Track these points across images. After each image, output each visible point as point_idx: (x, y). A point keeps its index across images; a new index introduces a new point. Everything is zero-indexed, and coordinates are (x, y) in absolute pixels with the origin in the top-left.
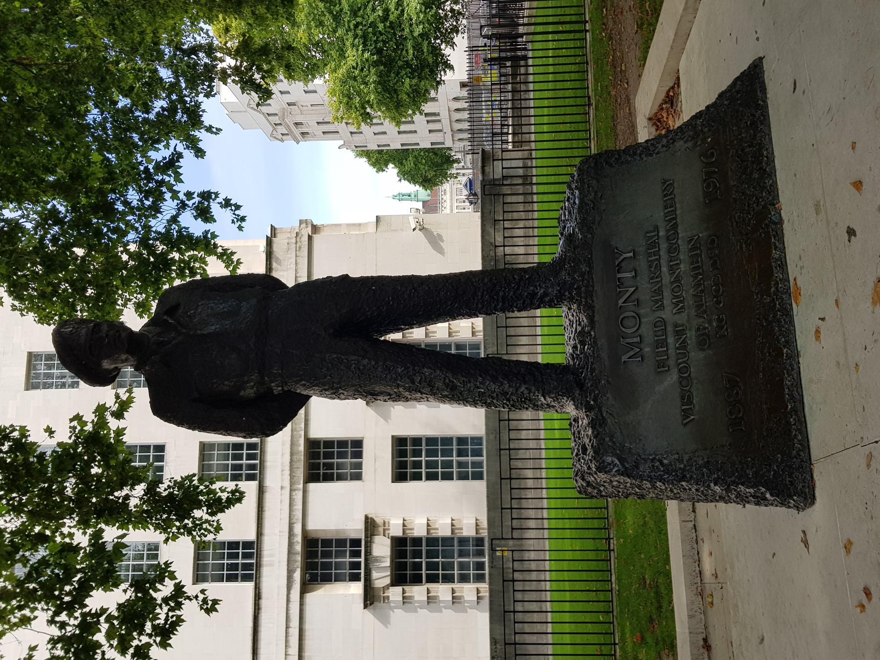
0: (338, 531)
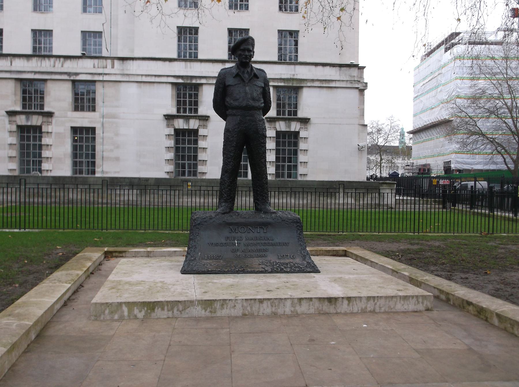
0: (201, 102)
